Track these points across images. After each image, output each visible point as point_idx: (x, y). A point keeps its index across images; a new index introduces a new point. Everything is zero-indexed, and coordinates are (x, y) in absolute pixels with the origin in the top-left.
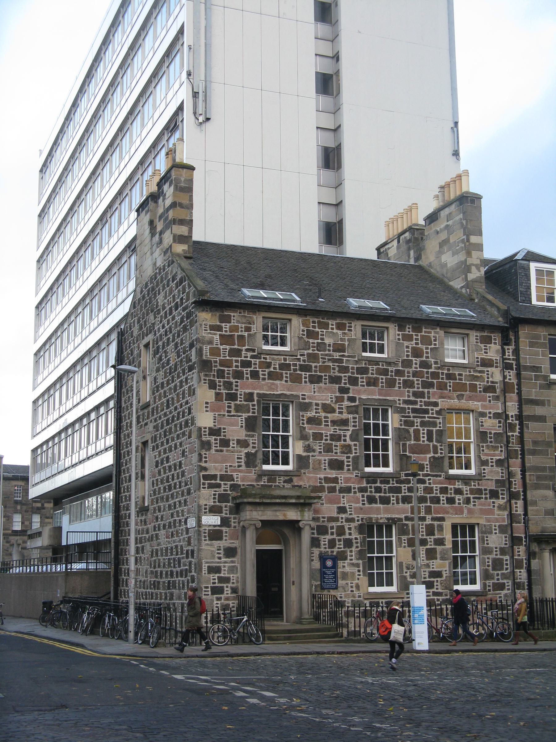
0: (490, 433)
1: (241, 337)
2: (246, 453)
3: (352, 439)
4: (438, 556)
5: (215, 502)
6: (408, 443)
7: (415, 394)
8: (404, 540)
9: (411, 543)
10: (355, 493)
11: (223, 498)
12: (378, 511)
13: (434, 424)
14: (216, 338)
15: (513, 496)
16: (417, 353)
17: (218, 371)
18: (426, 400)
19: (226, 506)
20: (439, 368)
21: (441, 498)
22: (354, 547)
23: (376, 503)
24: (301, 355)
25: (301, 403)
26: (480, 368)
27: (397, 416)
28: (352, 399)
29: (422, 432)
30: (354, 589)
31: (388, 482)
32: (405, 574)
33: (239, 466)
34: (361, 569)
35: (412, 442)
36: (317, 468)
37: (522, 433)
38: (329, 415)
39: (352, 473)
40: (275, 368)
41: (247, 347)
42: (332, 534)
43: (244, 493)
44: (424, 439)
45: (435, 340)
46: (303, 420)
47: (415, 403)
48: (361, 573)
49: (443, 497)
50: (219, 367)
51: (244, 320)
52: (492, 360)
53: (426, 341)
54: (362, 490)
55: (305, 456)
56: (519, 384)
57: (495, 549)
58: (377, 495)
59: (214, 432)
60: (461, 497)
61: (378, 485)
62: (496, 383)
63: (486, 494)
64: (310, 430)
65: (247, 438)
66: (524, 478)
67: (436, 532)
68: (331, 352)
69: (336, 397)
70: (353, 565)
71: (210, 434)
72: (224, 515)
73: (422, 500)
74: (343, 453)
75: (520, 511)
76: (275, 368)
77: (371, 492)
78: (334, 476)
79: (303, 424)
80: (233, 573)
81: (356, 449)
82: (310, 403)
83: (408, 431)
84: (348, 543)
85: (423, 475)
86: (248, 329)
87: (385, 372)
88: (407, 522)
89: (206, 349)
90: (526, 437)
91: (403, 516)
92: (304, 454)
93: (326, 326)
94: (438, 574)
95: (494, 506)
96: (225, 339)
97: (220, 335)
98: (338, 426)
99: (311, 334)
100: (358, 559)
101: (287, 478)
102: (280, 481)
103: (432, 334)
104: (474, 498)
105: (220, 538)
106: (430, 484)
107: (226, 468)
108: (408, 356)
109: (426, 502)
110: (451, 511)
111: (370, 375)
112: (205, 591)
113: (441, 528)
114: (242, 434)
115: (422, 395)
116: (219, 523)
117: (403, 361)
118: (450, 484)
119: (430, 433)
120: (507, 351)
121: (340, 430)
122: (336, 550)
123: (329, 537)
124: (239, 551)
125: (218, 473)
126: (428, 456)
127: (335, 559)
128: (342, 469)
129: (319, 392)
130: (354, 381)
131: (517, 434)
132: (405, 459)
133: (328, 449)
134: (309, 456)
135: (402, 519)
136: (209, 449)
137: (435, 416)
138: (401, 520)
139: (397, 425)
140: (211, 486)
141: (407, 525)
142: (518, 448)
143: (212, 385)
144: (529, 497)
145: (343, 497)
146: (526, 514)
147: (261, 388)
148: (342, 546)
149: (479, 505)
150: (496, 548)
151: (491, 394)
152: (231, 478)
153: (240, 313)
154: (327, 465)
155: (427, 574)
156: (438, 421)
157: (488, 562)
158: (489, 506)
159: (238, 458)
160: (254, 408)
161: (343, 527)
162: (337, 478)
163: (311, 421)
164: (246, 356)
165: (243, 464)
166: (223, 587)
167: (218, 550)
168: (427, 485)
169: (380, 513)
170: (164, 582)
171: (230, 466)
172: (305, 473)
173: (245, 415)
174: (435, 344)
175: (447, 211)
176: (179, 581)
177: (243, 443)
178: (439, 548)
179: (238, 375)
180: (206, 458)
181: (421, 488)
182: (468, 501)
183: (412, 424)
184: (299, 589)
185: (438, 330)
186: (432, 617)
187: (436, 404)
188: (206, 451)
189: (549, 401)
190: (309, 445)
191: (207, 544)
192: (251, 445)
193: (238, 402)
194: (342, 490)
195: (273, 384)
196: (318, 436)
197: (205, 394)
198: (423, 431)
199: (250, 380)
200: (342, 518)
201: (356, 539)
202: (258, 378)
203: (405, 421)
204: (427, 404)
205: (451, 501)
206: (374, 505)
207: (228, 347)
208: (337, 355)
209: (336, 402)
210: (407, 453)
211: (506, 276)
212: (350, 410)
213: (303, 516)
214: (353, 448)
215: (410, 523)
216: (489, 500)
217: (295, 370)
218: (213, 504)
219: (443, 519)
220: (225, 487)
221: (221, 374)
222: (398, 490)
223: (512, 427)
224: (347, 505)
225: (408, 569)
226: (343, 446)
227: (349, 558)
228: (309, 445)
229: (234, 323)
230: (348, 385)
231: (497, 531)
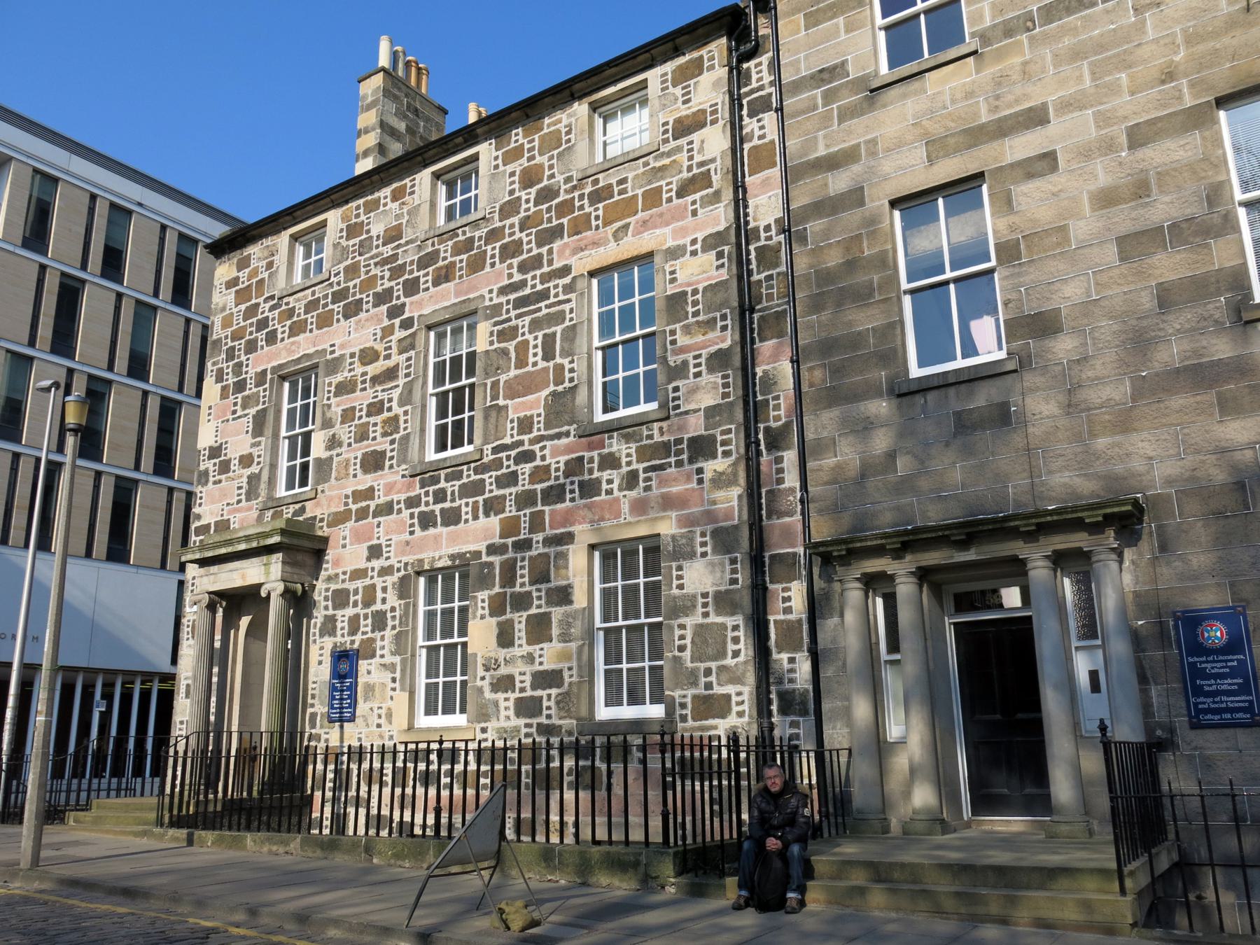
0: (695, 292)
3: (401, 404)
4: (555, 631)
8: (483, 601)
10: (400, 511)
13: (560, 318)
16: (529, 178)
20: (574, 188)
22: (389, 628)
30: (383, 721)
31: (459, 476)
34: (398, 675)
39: (398, 472)
42: (355, 604)
44: (535, 358)
45: (568, 133)
47: (523, 283)
48: (397, 685)
52: (704, 111)
55: (326, 459)
57: (700, 600)
60: (614, 474)
62: (713, 160)
77: (427, 504)
81: (406, 421)
83: (505, 352)
88: (491, 559)
94: (547, 679)
95: (700, 481)
98: (380, 383)
100: (393, 654)
101: (297, 506)
104: (646, 470)
115: (536, 262)
118: (591, 447)
120: (753, 71)
121: (383, 391)
122: (358, 638)
132: (494, 414)
135: (480, 553)
137: (562, 297)
141: (491, 564)
144: (810, 435)
145: (378, 526)
150: (705, 595)
151: (697, 196)
154: (358, 466)
155: (528, 678)
156: (567, 307)
157: (682, 637)
158: (689, 479)
161: (373, 586)
168: (538, 462)
178: (557, 613)
181: (523, 474)
186: (581, 794)
189: (873, 142)
198: (535, 340)
206: (432, 531)
210: (501, 402)
213: (267, 573)
215: (496, 560)
216: (687, 467)
222: (476, 488)
223: (768, 256)
224: (383, 541)
227: (379, 652)
230: (403, 299)
231: (709, 549)
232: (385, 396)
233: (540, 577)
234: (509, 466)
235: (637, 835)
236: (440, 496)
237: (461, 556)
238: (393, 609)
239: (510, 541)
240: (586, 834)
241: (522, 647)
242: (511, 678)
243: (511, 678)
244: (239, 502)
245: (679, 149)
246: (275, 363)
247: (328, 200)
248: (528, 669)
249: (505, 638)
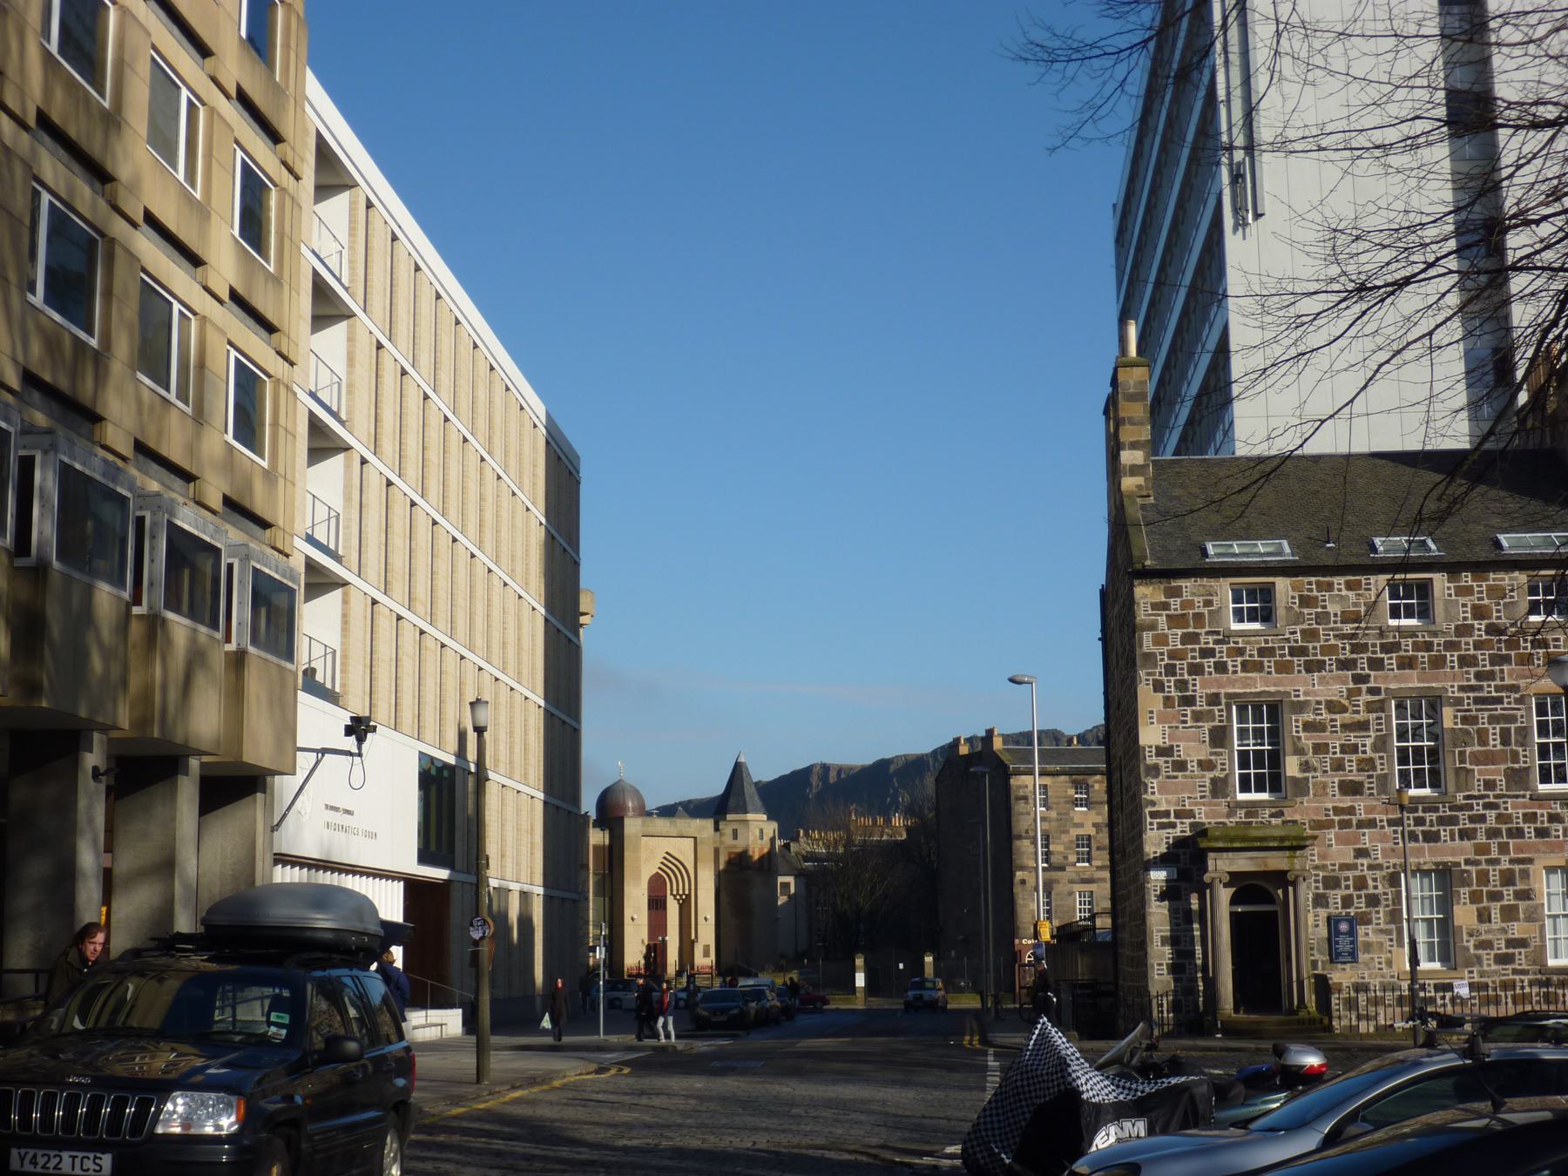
1: (1199, 617)
6: (1468, 750)
9: (1475, 898)
12: (1420, 852)
13: (1513, 719)
14: (1162, 621)
16: (1479, 612)
18: (1498, 682)
28: (1374, 691)
31: (1436, 810)
35: (1477, 748)
38: (1337, 716)
42: (1347, 887)
44: (1495, 743)
47: (1480, 688)
49: (1529, 829)
59: (1163, 751)
61: (1420, 814)
70: (1382, 931)
71: (1157, 755)
73: (1493, 833)
82: (1306, 703)
84: (1373, 901)
85: (1496, 797)
86: (1208, 603)
87: (1428, 646)
93: (1330, 587)
96: (1174, 621)
99: (1306, 601)
108: (1465, 619)
110: (1543, 848)
113: (1525, 875)
114: (1204, 752)
115: (1490, 676)
118: (1540, 807)
122: (1352, 911)
127: (1353, 922)
130: (1376, 664)
133: (1338, 766)
138: (1458, 864)
140: (1161, 826)
143: (1158, 687)
147: (1232, 683)
156: (1519, 713)
162: (1353, 808)
163: (1308, 727)
164: (1208, 641)
173: (1207, 726)
177: (1206, 765)
178: (1522, 905)
179: (1196, 670)
190: (1307, 762)
194: (1361, 824)
204: (1498, 689)
207: (1180, 632)
208: (1348, 628)
210: (1468, 766)
212: (1370, 707)
214: (1378, 762)
215: (1473, 869)
217: (1283, 655)
219: (1530, 861)
221: (1171, 671)
222: (1453, 821)
225: (1471, 935)
226: (1360, 761)
228: (1307, 762)
229: (1186, 596)
232: (1359, 741)
237: (1445, 864)
246: (1231, 691)
248: (1503, 937)
249: (1484, 916)
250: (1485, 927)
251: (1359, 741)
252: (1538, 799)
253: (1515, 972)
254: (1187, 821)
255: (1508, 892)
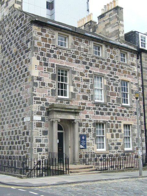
1: (50, 40)
2: (51, 89)
5: (39, 110)
6: (109, 91)
7: (111, 73)
10: (92, 110)
11: (42, 108)
12: (100, 118)
14: (40, 37)
15: (141, 115)
17: (41, 52)
19: (44, 112)
21: (120, 114)
22: (92, 132)
23: (99, 114)
24: (72, 51)
25: (72, 70)
26: (131, 66)
27: (105, 80)
28: (90, 72)
29: (113, 87)
31: (103, 107)
32: (109, 144)
33: (49, 95)
34: (94, 141)
35: (111, 91)
36: (78, 99)
37: (143, 91)
38: (82, 77)
40: (62, 55)
41: (52, 44)
43: (52, 106)
44: (114, 90)
45: (117, 53)
46: (73, 78)
47: (111, 76)
48: (94, 143)
49: (121, 114)
50: (41, 51)
51: (51, 33)
53: (115, 53)
54: (94, 109)
56: (142, 73)
58: (99, 111)
59: (39, 79)
61: (99, 107)
62: (136, 72)
63: (134, 113)
64: (76, 82)
65: (52, 83)
66: (144, 108)
67: (119, 127)
68: (83, 52)
69: (85, 70)
72: (42, 116)
73: (114, 114)
74: (87, 93)
75: (143, 121)
76: (62, 55)
78: (85, 102)
79: (73, 79)
80: (46, 142)
83: (109, 87)
84: (90, 130)
86: (53, 37)
87: (101, 63)
88: (109, 123)
89: (36, 42)
90: (145, 94)
91: (108, 120)
92: (74, 92)
93: (81, 41)
94: (119, 144)
97: (42, 37)
98: (86, 82)
101: (67, 102)
102: (65, 102)
103: (116, 51)
105: (41, 127)
106: (116, 108)
107: (44, 95)
109: (115, 115)
111: (96, 63)
112: (35, 150)
116: (41, 120)
117: (107, 59)
119: (116, 88)
121: (86, 83)
123: (83, 128)
124: (49, 132)
125: (40, 97)
126: (116, 97)
128: (87, 100)
129: (79, 67)
130: (91, 64)
131: (141, 92)
133: (82, 91)
134: (75, 93)
136: (37, 86)
137: (117, 82)
138: (107, 121)
139: (105, 84)
140: (37, 103)
142: (142, 97)
143: (38, 58)
146: (145, 122)
148: (87, 132)
149: (132, 117)
152: (45, 100)
153: (50, 29)
154: (82, 97)
159: (48, 91)
160: (55, 71)
161: (88, 123)
162: (85, 103)
163: (76, 78)
165: (50, 94)
166: (42, 148)
167: (40, 132)
169: (101, 119)
170: (7, 147)
171: (45, 95)
172: (74, 100)
173: (51, 73)
174: (117, 55)
175: (109, 13)
176: (18, 146)
177: (50, 85)
179: (49, 55)
180: (35, 90)
182: (128, 115)
183: (110, 84)
184: (73, 148)
185: (118, 49)
187: (118, 77)
188: (36, 87)
191: (36, 129)
192: (54, 86)
193: (48, 67)
195: (62, 61)
196: (78, 85)
197: (35, 62)
198: (114, 87)
199: (53, 58)
200: (87, 120)
201: (92, 129)
202: (56, 58)
203: (108, 83)
205: (123, 115)
206: (98, 115)
207: (45, 43)
208: (85, 53)
209: (85, 72)
210: (109, 95)
211: (131, 37)
214: (91, 91)
217: (70, 57)
218: (38, 111)
219: (120, 122)
220: (43, 104)
224: (89, 115)
226: (88, 90)
227: (90, 136)
229: (47, 33)
230: (89, 66)
232: (87, 85)
233: (117, 127)
234: (111, 108)
235: (129, 166)
236: (100, 109)
238: (92, 129)
239: (112, 120)
240: (125, 167)
241: (115, 138)
242: (113, 143)
243: (113, 143)
244: (49, 95)
245: (132, 67)
247: (71, 32)
249: (112, 136)
250: (112, 139)
251: (87, 85)
252: (123, 106)
253: (119, 152)
254: (45, 102)
255: (117, 130)
